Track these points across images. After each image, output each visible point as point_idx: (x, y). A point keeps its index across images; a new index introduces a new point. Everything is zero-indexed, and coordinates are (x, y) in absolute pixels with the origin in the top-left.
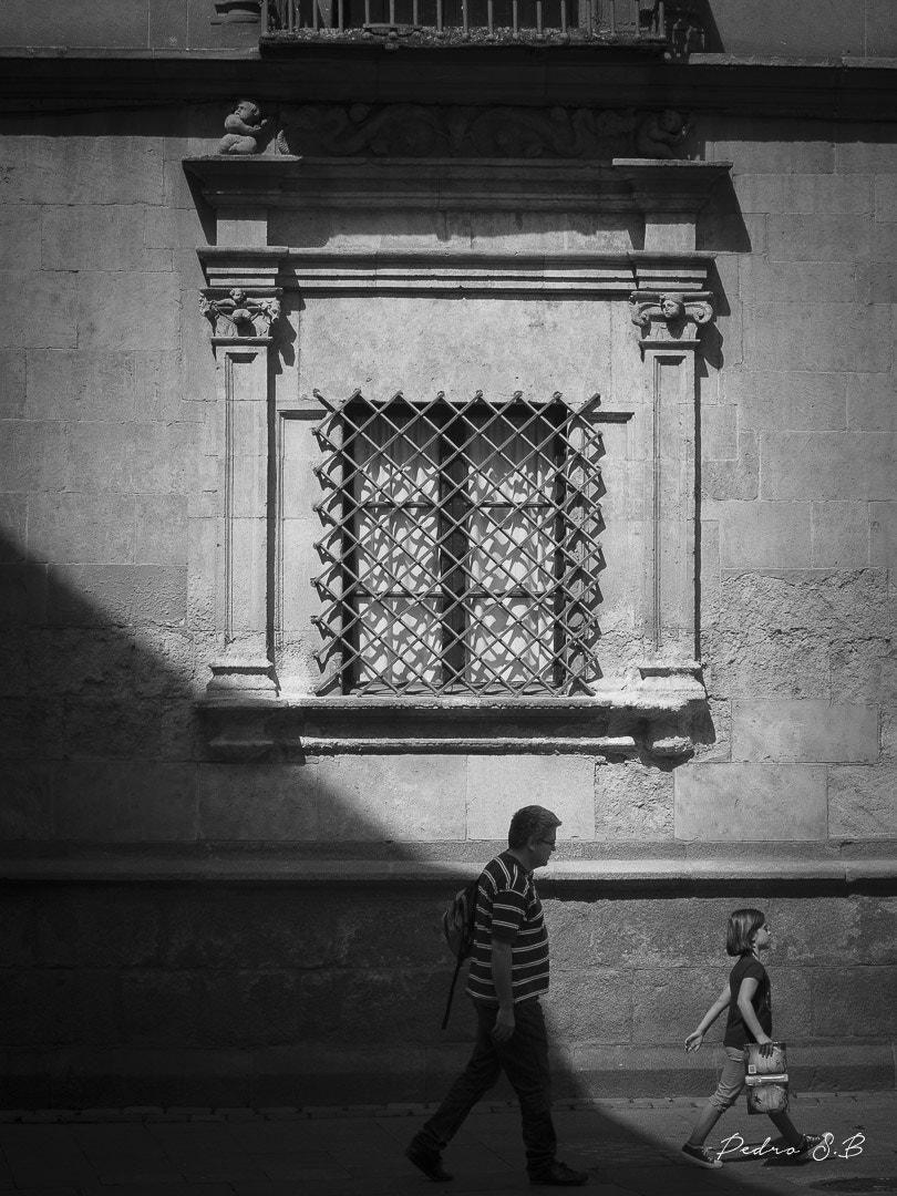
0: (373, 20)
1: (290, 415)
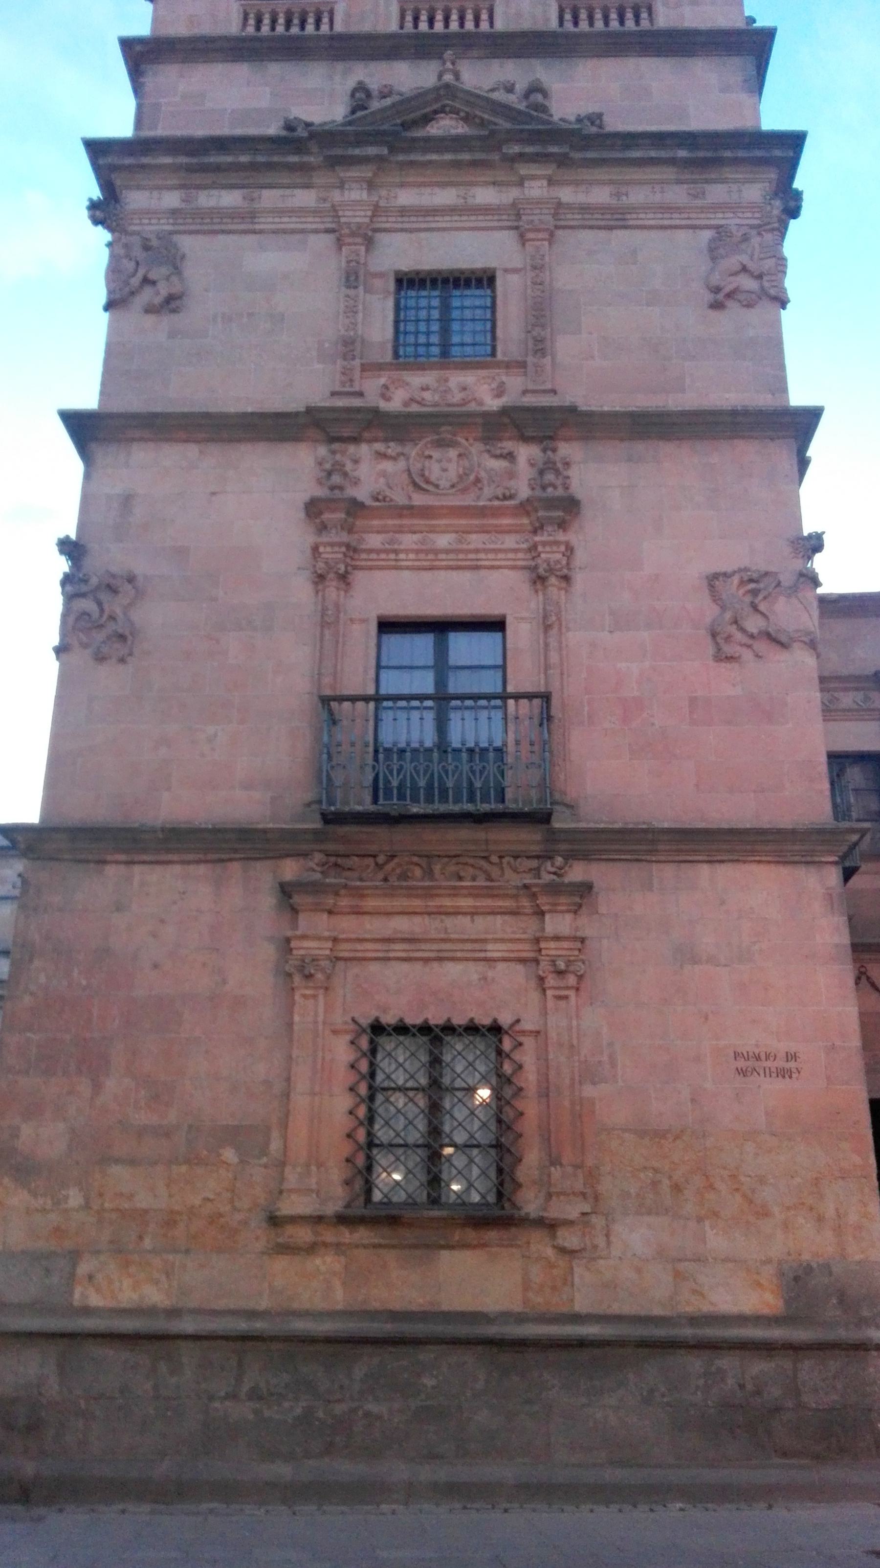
0: (385, 799)
1: (335, 1032)
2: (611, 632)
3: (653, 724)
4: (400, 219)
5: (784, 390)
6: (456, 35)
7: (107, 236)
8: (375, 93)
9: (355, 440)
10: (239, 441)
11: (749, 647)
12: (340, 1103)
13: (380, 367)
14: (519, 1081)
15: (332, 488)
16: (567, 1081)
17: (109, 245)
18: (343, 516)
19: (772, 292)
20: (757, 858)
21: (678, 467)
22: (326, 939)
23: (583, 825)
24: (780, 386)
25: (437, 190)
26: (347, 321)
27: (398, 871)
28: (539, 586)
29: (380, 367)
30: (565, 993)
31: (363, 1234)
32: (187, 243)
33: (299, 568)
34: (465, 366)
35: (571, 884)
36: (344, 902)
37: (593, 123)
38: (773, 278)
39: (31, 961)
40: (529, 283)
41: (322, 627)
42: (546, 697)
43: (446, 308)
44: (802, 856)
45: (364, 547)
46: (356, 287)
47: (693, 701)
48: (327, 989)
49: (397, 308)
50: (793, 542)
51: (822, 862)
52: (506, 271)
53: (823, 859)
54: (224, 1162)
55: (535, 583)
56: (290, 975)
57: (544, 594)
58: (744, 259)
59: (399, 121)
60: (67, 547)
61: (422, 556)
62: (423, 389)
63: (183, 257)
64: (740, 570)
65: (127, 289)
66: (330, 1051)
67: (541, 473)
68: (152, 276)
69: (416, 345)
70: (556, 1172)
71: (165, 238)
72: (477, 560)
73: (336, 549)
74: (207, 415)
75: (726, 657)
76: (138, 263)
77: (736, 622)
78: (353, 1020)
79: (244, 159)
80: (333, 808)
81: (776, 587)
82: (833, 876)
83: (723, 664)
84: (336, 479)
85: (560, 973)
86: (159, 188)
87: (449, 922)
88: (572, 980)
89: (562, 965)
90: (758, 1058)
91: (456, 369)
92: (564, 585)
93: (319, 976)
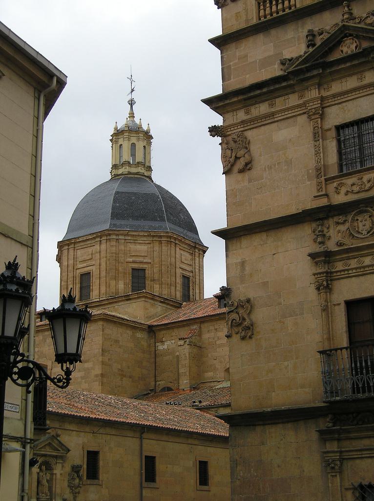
1: (347, 489)
4: (333, 100)
8: (316, 33)
10: (281, 227)
22: (337, 452)
49: (339, 142)
59: (327, 49)
66: (345, 497)
73: (322, 275)
93: (337, 467)
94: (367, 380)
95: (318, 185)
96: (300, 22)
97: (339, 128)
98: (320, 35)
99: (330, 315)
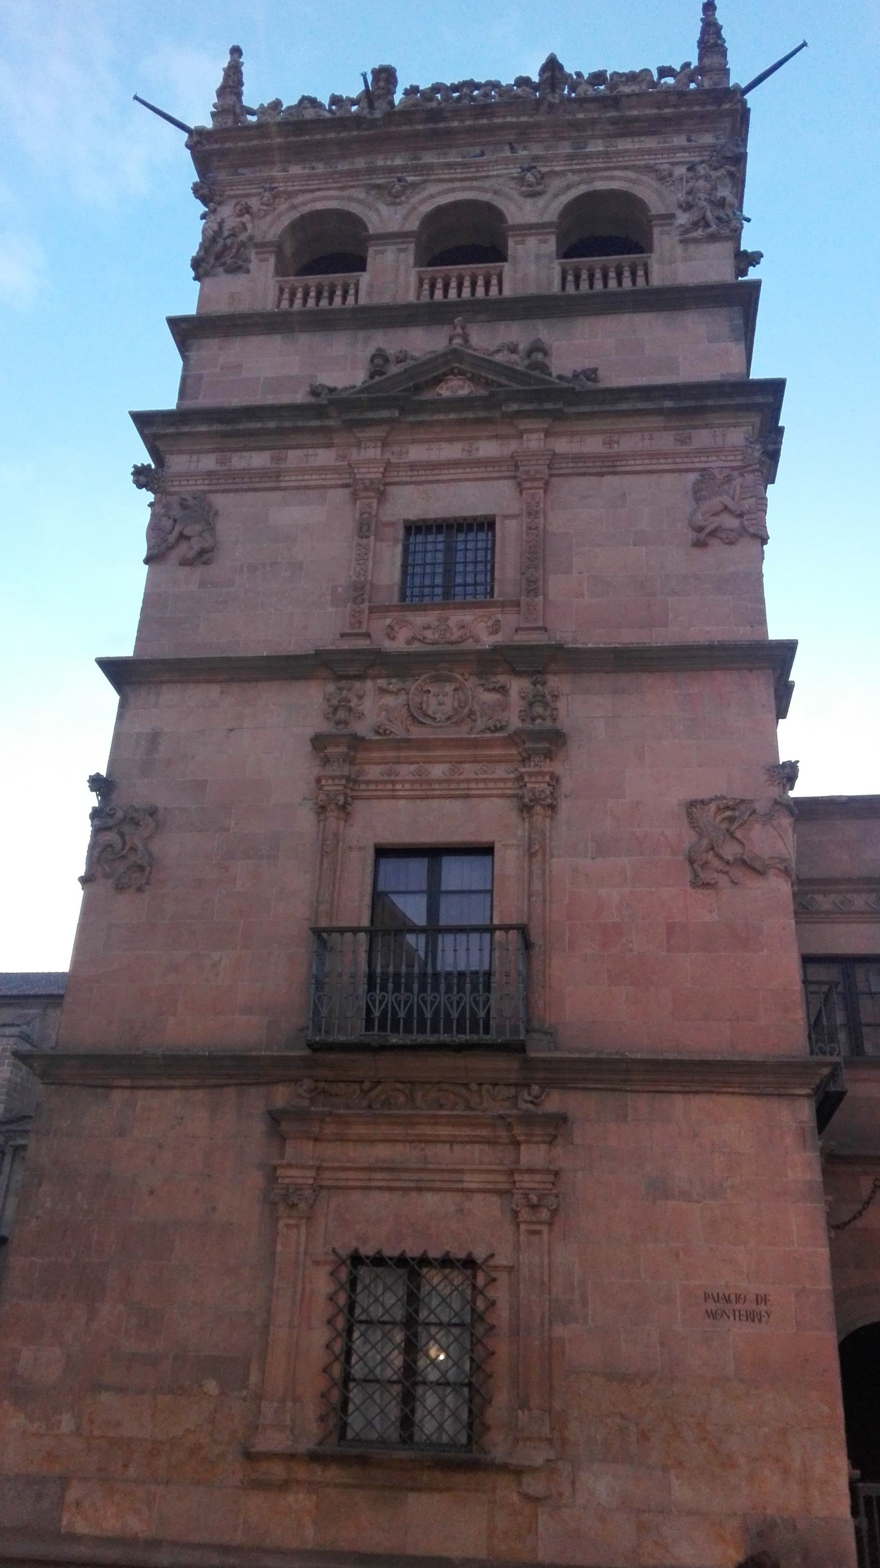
1: (317, 1263)
2: (593, 858)
3: (631, 950)
5: (763, 622)
6: (465, 303)
7: (150, 497)
8: (392, 359)
9: (361, 677)
10: (257, 680)
11: (726, 873)
12: (318, 1337)
13: (387, 609)
14: (491, 1319)
15: (338, 723)
16: (538, 1320)
17: (151, 505)
18: (346, 750)
19: (752, 530)
20: (730, 1090)
21: (658, 702)
22: (311, 1167)
23: (558, 1055)
24: (759, 617)
25: (444, 445)
26: (358, 568)
27: (383, 1097)
28: (525, 814)
29: (387, 609)
30: (537, 1227)
31: (334, 1473)
32: (219, 501)
33: (304, 799)
34: (463, 606)
35: (544, 1115)
36: (330, 1129)
37: (588, 379)
38: (754, 516)
39: (40, 1184)
40: (524, 528)
41: (322, 856)
42: (523, 930)
43: (450, 550)
44: (776, 1088)
45: (362, 778)
46: (367, 537)
47: (670, 928)
48: (309, 1218)
50: (769, 770)
51: (793, 1095)
52: (505, 517)
53: (797, 1092)
54: (205, 1393)
55: (522, 811)
56: (275, 1204)
57: (530, 822)
58: (726, 499)
59: (411, 384)
60: (96, 783)
61: (417, 786)
62: (424, 628)
63: (216, 514)
64: (716, 798)
65: (164, 546)
66: (311, 1282)
67: (531, 704)
68: (187, 532)
69: (422, 586)
70: (523, 1416)
71: (201, 498)
72: (469, 789)
73: (337, 782)
74: (228, 659)
75: (703, 884)
76: (175, 521)
77: (713, 849)
78: (334, 1250)
79: (272, 425)
80: (318, 1039)
81: (750, 815)
82: (806, 1111)
83: (700, 891)
84: (341, 714)
85: (534, 1207)
86: (199, 452)
87: (430, 1150)
88: (544, 1214)
89: (534, 1199)
90: (728, 1300)
91: (455, 608)
92: (549, 812)
93: (303, 1206)
94: (418, 1003)
95: (353, 616)
96: (361, 334)
97: (413, 528)
98: (399, 362)
99: (339, 868)
